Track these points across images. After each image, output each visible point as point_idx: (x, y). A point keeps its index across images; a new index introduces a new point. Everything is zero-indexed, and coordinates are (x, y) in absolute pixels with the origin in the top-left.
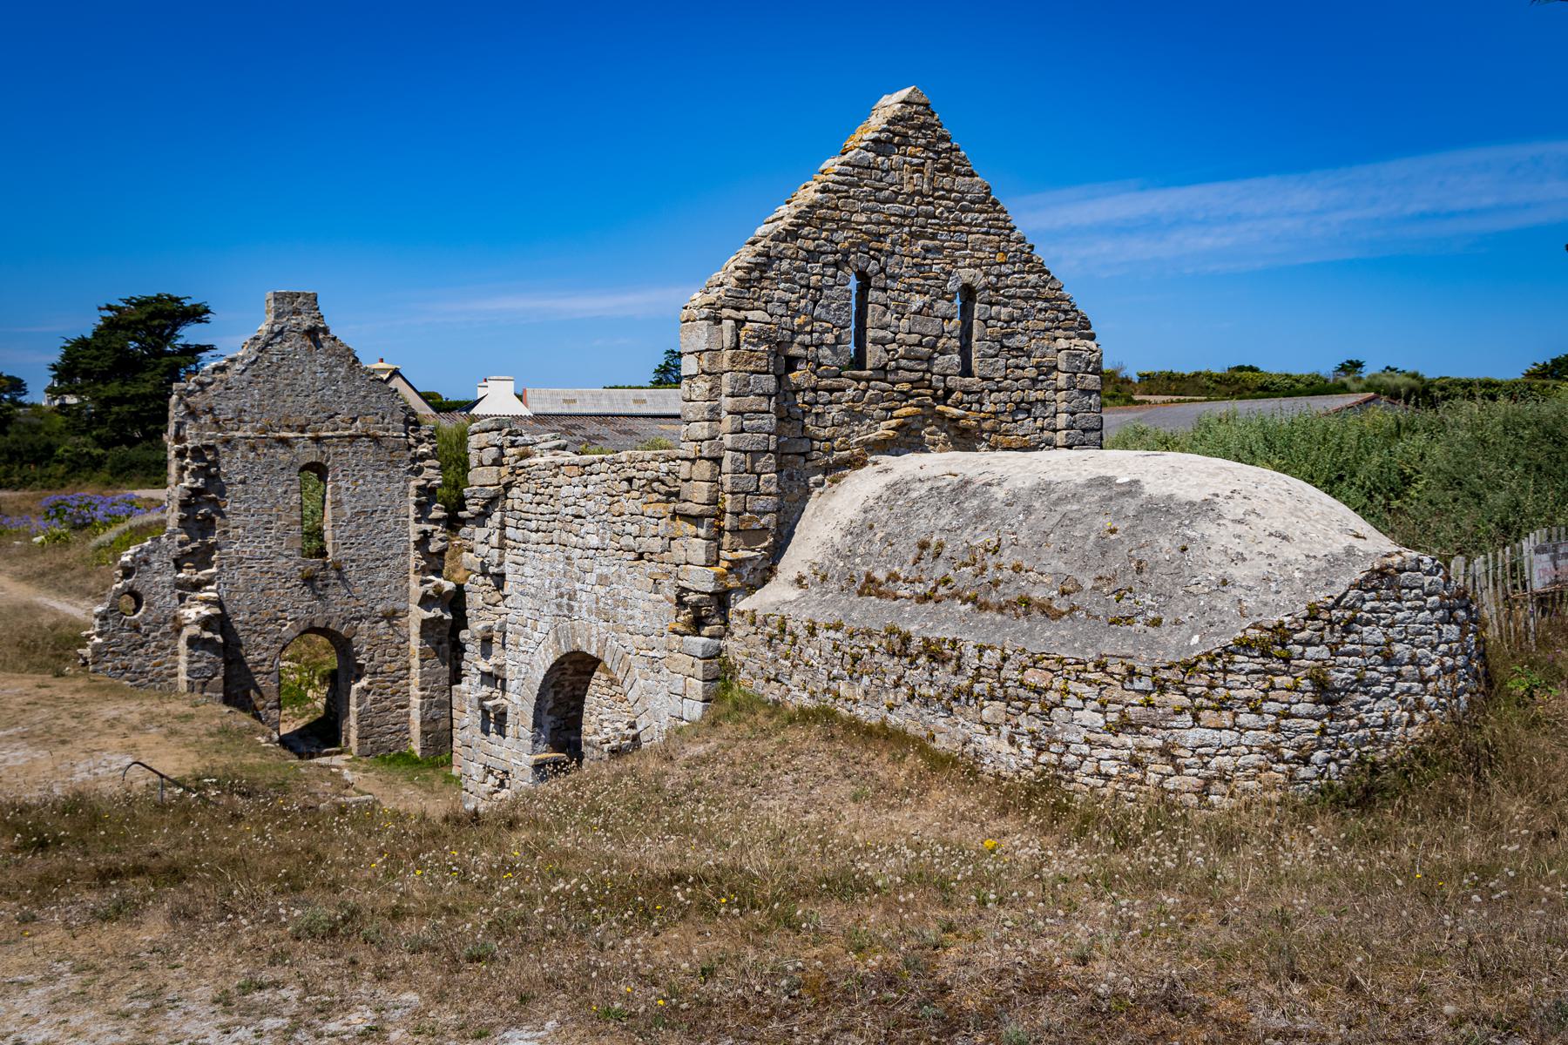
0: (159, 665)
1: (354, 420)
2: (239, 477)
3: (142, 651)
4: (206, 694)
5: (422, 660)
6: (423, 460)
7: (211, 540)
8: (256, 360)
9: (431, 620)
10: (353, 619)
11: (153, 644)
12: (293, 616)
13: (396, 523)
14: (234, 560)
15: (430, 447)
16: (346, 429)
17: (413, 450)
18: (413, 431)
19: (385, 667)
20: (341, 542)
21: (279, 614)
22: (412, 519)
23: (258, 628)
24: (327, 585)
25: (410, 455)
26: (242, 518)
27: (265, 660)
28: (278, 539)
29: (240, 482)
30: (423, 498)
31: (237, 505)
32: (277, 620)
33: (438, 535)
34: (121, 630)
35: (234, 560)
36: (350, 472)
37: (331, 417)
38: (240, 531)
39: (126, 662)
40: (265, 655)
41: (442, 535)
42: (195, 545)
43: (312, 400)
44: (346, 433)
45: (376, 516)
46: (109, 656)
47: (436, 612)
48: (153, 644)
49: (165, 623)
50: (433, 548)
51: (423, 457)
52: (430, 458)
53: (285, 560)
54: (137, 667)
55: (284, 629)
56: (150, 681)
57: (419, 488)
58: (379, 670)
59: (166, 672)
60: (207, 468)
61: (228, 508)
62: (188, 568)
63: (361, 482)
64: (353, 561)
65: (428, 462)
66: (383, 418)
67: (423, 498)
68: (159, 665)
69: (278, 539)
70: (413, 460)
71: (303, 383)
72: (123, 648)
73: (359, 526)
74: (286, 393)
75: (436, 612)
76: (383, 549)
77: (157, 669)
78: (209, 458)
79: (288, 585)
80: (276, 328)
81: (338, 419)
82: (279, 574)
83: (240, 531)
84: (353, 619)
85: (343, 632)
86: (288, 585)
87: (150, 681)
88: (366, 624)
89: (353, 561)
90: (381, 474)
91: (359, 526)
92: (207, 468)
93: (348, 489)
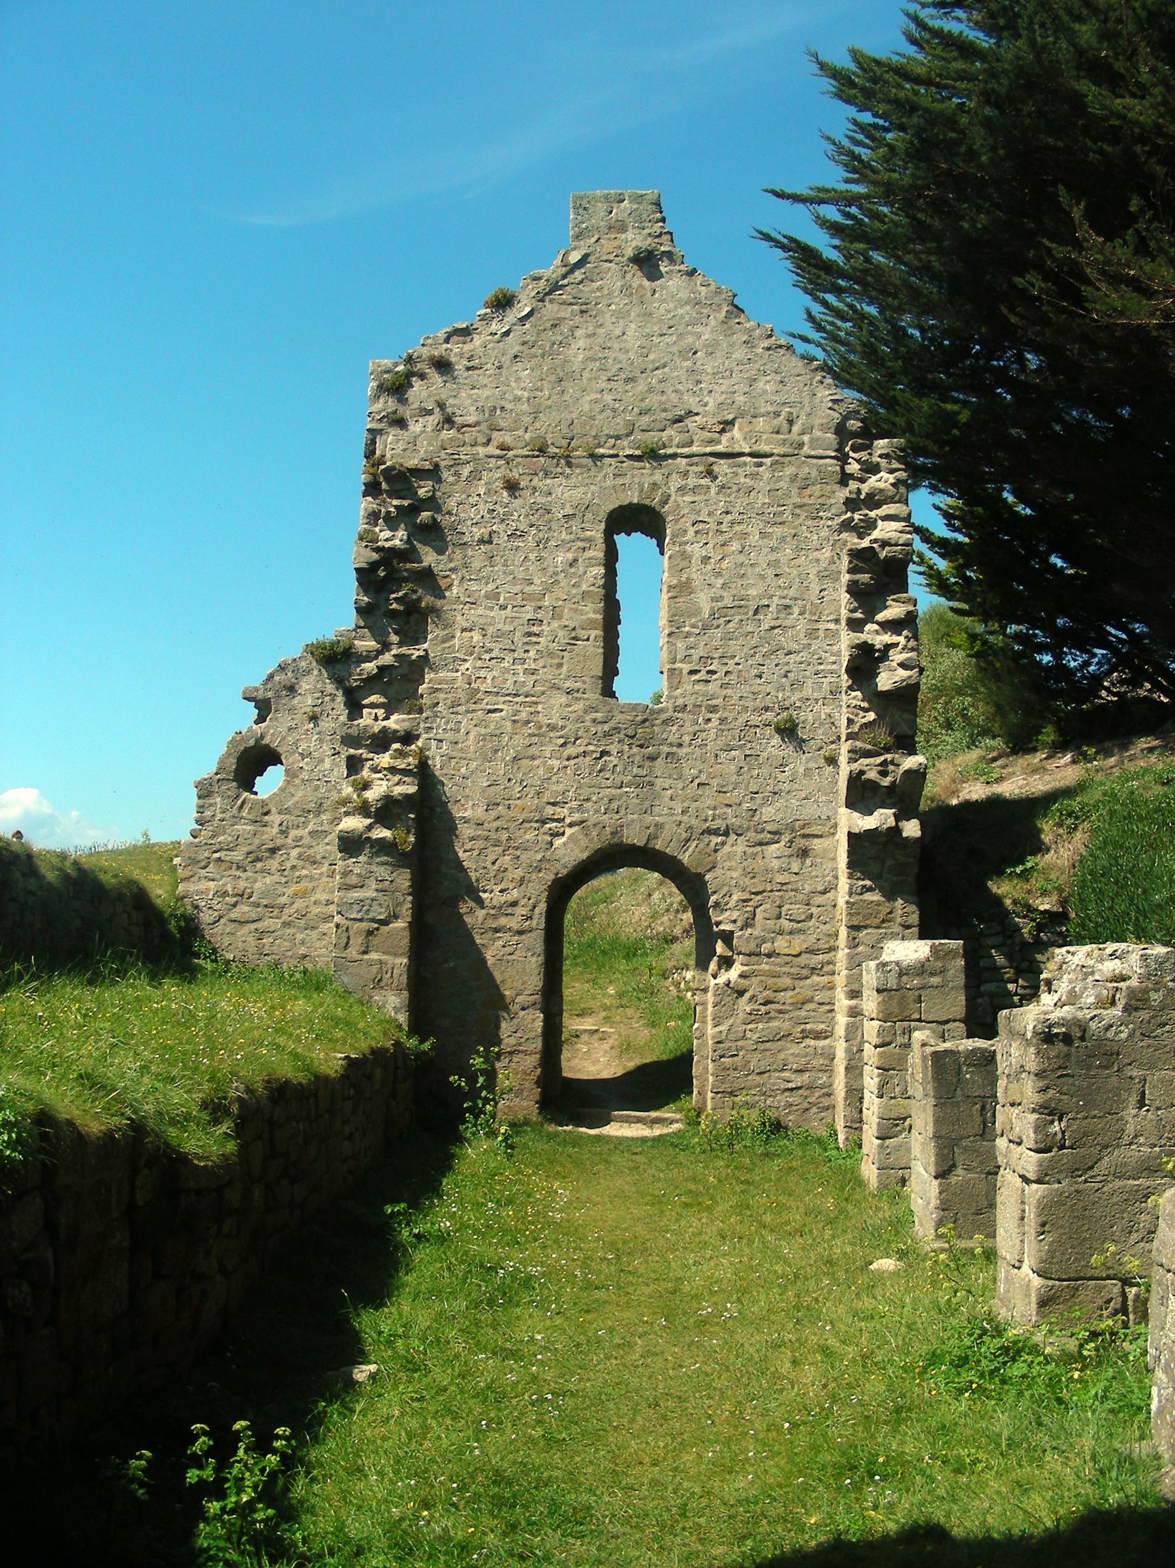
0: (304, 894)
1: (727, 425)
2: (478, 532)
3: (274, 864)
4: (374, 956)
5: (854, 928)
6: (878, 505)
7: (416, 653)
8: (530, 314)
9: (871, 834)
10: (709, 832)
11: (294, 853)
12: (577, 817)
13: (812, 633)
14: (461, 695)
15: (891, 478)
16: (711, 442)
17: (853, 485)
18: (855, 449)
19: (781, 944)
20: (686, 667)
21: (550, 810)
22: (843, 623)
23: (504, 836)
24: (653, 758)
25: (843, 494)
26: (480, 611)
27: (514, 904)
28: (551, 655)
29: (481, 541)
30: (865, 578)
31: (474, 587)
32: (544, 822)
33: (896, 657)
34: (237, 819)
35: (461, 695)
36: (713, 526)
37: (679, 420)
38: (476, 637)
39: (242, 884)
40: (515, 894)
41: (905, 656)
42: (387, 659)
43: (641, 387)
44: (708, 450)
45: (767, 621)
46: (211, 868)
47: (881, 818)
48: (294, 853)
49: (318, 814)
50: (886, 680)
51: (873, 500)
52: (890, 500)
53: (563, 699)
54: (264, 895)
55: (558, 842)
56: (286, 924)
57: (855, 554)
58: (766, 948)
59: (316, 910)
60: (414, 510)
61: (455, 590)
62: (373, 706)
63: (735, 546)
64: (713, 709)
65: (885, 510)
66: (791, 422)
67: (865, 578)
68: (304, 894)
69: (551, 655)
70: (852, 504)
71: (621, 356)
72: (238, 855)
73: (728, 637)
74: (586, 375)
75: (881, 818)
76: (781, 688)
77: (299, 904)
78: (421, 492)
79: (571, 750)
80: (574, 257)
81: (691, 423)
82: (551, 727)
83: (476, 637)
84: (709, 832)
85: (685, 858)
86: (571, 750)
87: (286, 924)
88: (736, 847)
89: (713, 709)
90: (778, 531)
91: (728, 637)
92: (414, 510)
93: (706, 559)
